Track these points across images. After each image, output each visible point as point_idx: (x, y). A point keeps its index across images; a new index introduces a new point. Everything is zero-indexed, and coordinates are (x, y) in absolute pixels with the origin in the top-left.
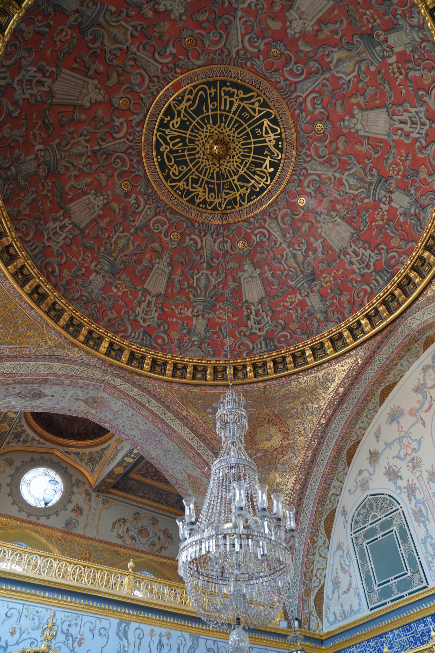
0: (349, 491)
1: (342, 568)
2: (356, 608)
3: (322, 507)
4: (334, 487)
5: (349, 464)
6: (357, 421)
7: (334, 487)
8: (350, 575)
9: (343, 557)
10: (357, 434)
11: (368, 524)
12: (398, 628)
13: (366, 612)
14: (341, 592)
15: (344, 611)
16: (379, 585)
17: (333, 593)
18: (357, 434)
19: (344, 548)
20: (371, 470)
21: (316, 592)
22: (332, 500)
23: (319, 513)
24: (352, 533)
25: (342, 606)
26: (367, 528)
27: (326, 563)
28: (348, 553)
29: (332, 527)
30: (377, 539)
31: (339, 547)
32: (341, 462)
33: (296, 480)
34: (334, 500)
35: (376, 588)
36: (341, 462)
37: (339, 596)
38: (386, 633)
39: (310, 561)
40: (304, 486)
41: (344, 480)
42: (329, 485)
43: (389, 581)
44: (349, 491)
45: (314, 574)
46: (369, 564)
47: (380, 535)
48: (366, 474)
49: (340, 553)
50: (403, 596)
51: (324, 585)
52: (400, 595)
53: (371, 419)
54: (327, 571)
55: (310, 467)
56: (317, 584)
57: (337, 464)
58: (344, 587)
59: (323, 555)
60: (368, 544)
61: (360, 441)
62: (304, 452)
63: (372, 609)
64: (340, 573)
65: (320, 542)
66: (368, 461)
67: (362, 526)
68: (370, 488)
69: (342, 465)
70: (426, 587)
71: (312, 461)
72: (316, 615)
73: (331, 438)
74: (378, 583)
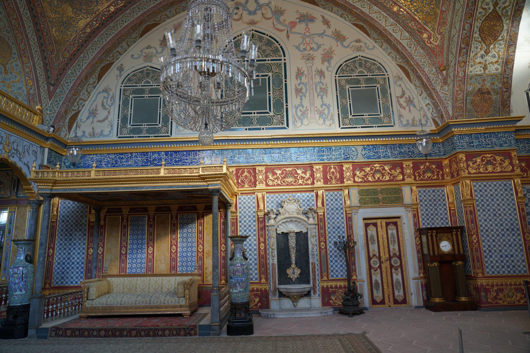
0: (133, 55)
1: (103, 105)
2: (106, 132)
4: (122, 47)
5: (141, 35)
6: (168, 9)
8: (109, 112)
9: (107, 98)
10: (160, 18)
11: (140, 85)
12: (137, 153)
13: (113, 138)
14: (95, 120)
15: (94, 133)
16: (132, 125)
17: (88, 118)
18: (160, 18)
19: (111, 93)
20: (160, 50)
21: (73, 113)
23: (101, 60)
24: (123, 85)
25: (93, 129)
26: (138, 87)
27: (88, 98)
28: (113, 97)
29: (104, 75)
30: (144, 97)
31: (105, 91)
32: (137, 31)
34: (117, 56)
35: (129, 126)
36: (137, 31)
37: (92, 122)
38: (127, 153)
40: (94, 32)
41: (131, 45)
42: (119, 43)
43: (142, 125)
44: (133, 55)
45: (77, 101)
46: (130, 110)
47: (147, 96)
48: (154, 51)
49: (105, 95)
50: (149, 137)
51: (80, 111)
52: (147, 135)
53: (177, 13)
54: (87, 103)
55: (107, 20)
56: (76, 108)
57: (133, 31)
58: (100, 117)
60: (134, 97)
61: (159, 24)
62: (108, 4)
63: (119, 137)
64: (100, 108)
65: (91, 81)
66: (159, 43)
67: (134, 85)
68: (153, 62)
69: (136, 33)
70: (169, 136)
71: (111, 17)
72: (67, 128)
73: (139, 9)
74: (131, 124)
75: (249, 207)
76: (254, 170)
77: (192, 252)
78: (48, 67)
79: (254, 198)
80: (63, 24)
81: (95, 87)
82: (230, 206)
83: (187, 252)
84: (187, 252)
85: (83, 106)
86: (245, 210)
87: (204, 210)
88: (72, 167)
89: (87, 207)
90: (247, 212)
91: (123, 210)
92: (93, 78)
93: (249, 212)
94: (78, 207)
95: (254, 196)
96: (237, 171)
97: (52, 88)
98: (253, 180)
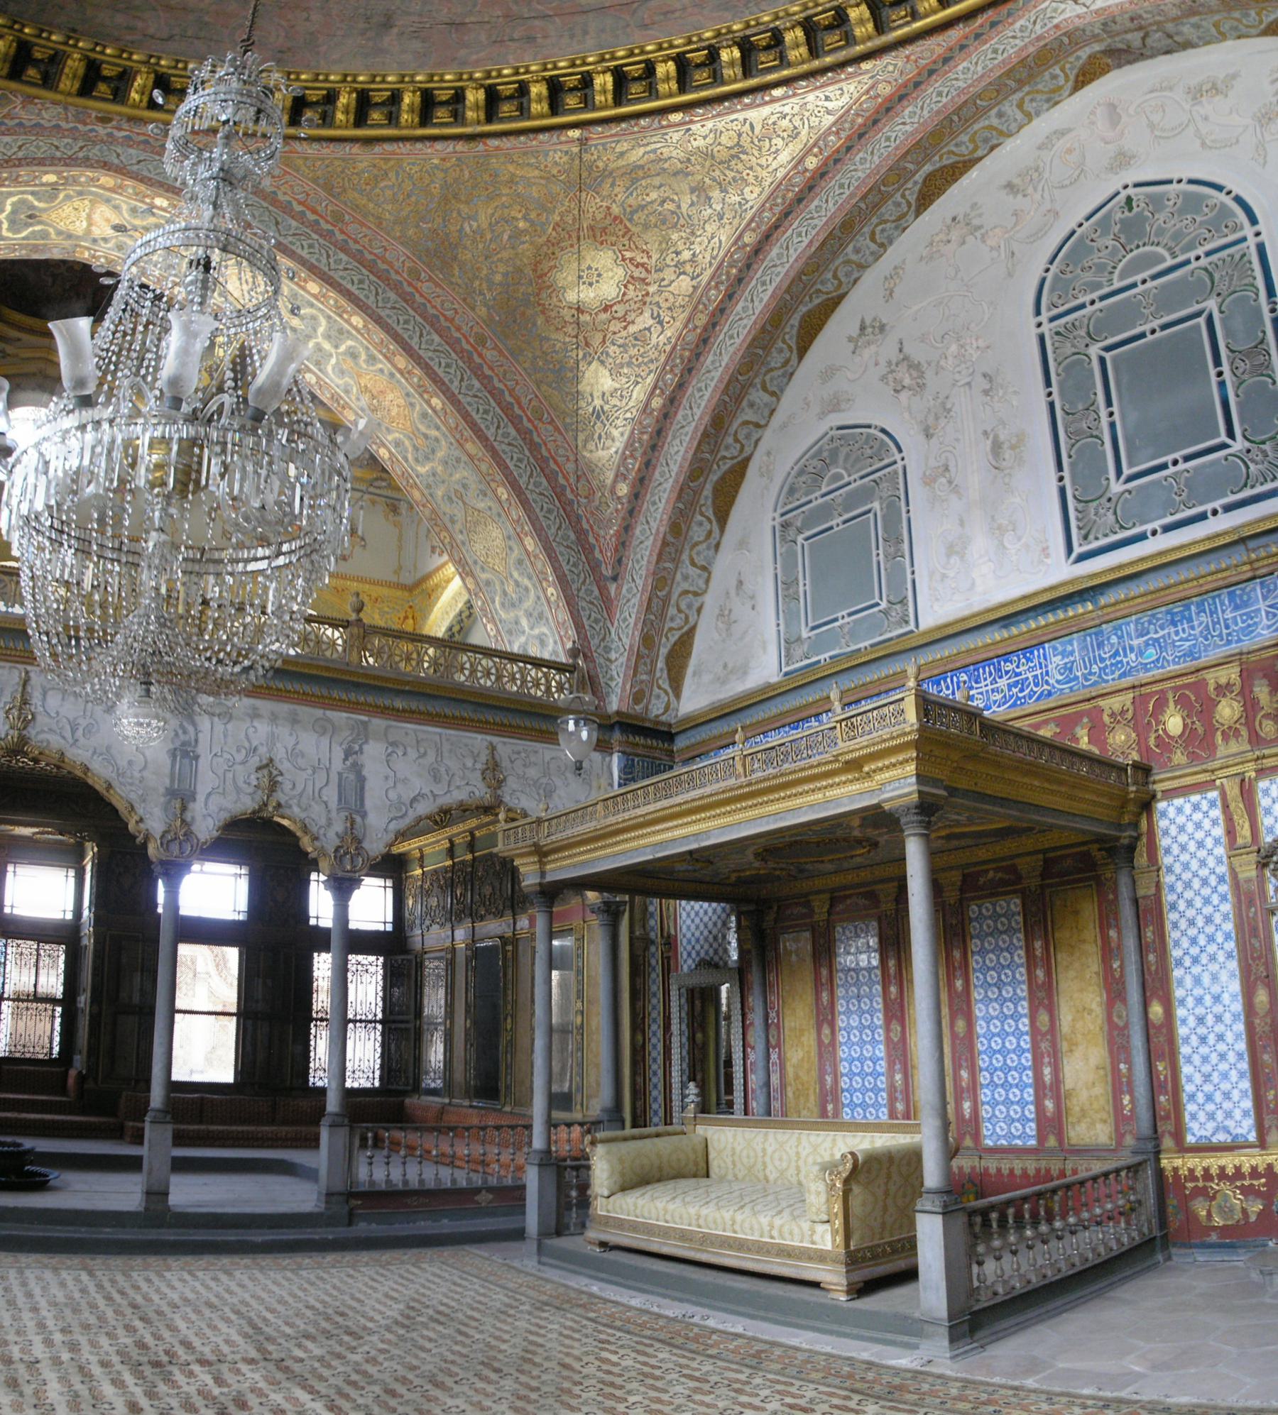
3: (712, 452)
4: (752, 405)
7: (752, 405)
16: (813, 628)
21: (673, 640)
22: (741, 437)
24: (777, 515)
27: (707, 581)
33: (655, 387)
34: (748, 437)
35: (805, 634)
39: (665, 574)
42: (738, 400)
43: (836, 620)
51: (693, 629)
54: (709, 600)
56: (678, 622)
59: (700, 561)
60: (807, 539)
63: (786, 674)
65: (697, 533)
72: (666, 686)
75: (1200, 845)
76: (1204, 683)
78: (592, 540)
79: (1212, 804)
80: (598, 417)
81: (717, 546)
82: (1131, 849)
83: (1003, 1034)
85: (699, 610)
86: (1185, 857)
87: (1043, 876)
90: (1194, 865)
91: (816, 904)
92: (701, 524)
93: (1203, 863)
95: (1213, 794)
96: (1139, 702)
97: (613, 588)
98: (1201, 731)
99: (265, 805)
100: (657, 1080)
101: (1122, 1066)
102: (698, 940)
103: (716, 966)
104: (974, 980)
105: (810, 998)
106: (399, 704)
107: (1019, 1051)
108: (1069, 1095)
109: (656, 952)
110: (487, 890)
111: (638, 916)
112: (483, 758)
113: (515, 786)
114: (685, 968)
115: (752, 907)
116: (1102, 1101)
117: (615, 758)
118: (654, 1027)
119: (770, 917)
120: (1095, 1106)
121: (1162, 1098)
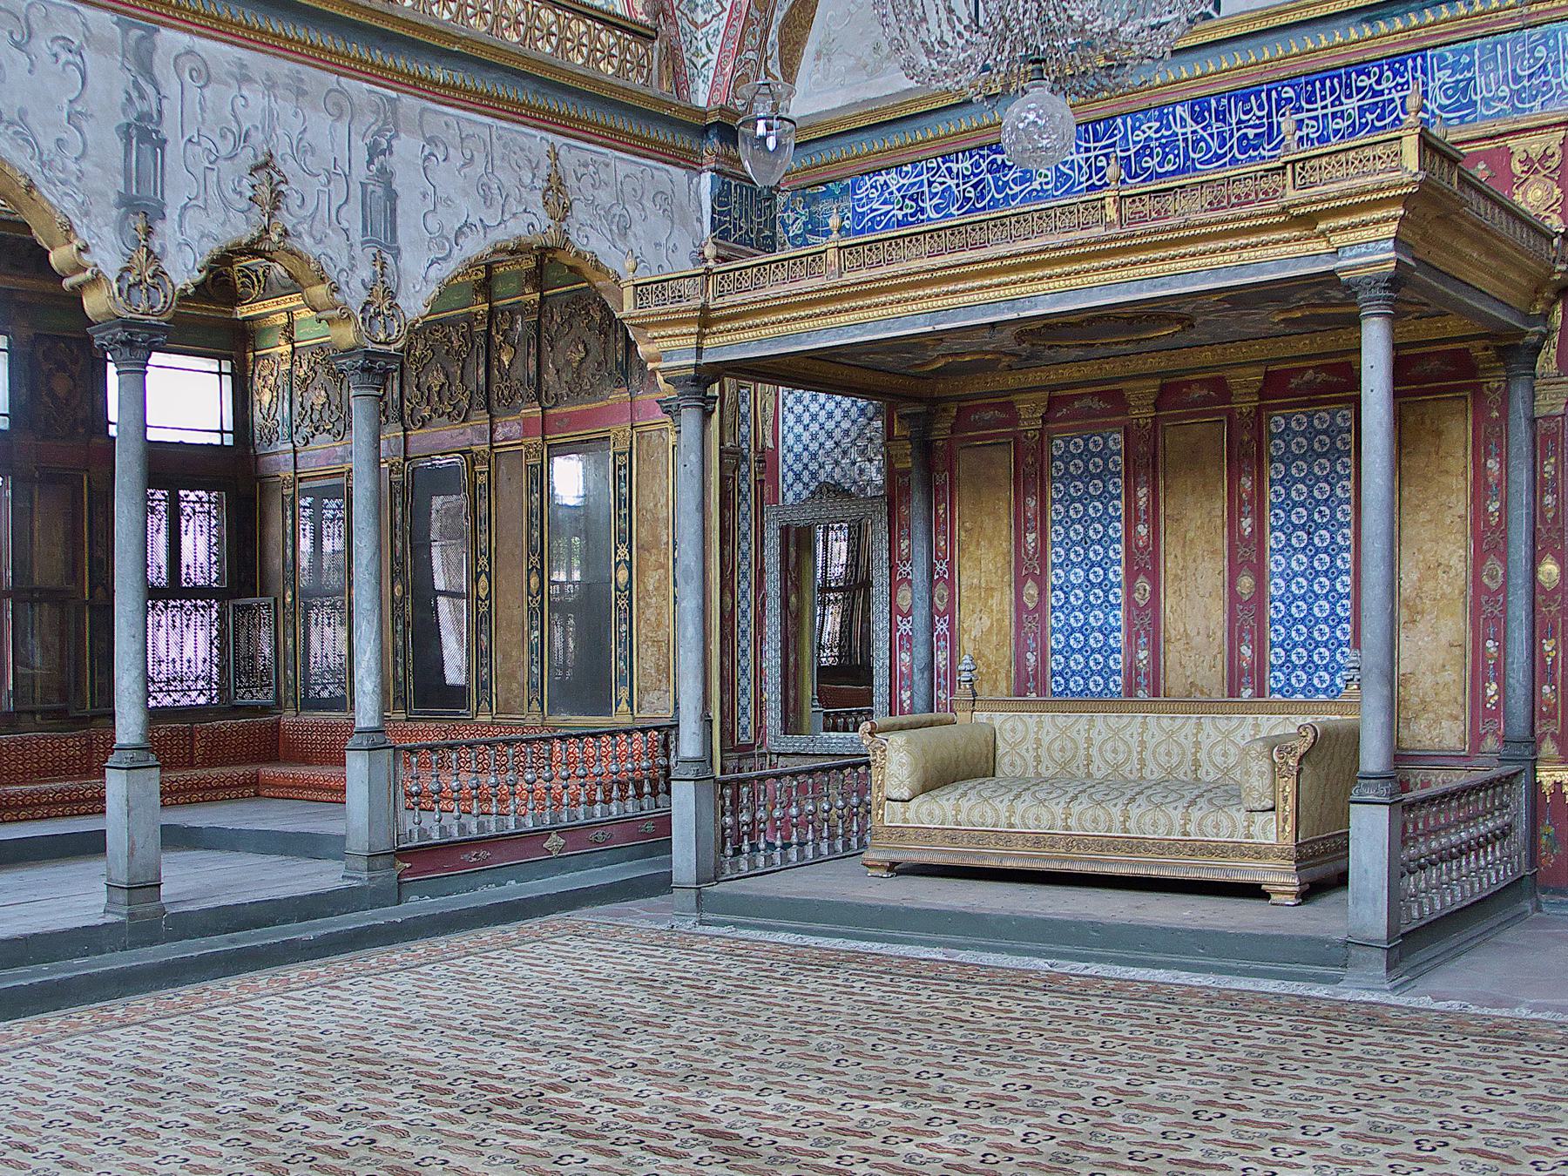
77: (1333, 596)
83: (1311, 597)
84: (1311, 597)
88: (811, 239)
89: (878, 412)
94: (846, 413)
99: (267, 232)
100: (747, 662)
101: (1490, 643)
102: (814, 456)
103: (847, 493)
104: (1270, 520)
105: (1005, 544)
106: (440, 74)
107: (1334, 620)
108: (1405, 681)
109: (749, 473)
110: (436, 379)
111: (729, 420)
112: (544, 172)
113: (582, 217)
114: (790, 496)
115: (921, 409)
116: (1455, 691)
117: (706, 178)
118: (744, 585)
119: (941, 430)
120: (1444, 696)
121: (1546, 689)
